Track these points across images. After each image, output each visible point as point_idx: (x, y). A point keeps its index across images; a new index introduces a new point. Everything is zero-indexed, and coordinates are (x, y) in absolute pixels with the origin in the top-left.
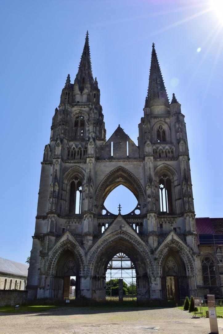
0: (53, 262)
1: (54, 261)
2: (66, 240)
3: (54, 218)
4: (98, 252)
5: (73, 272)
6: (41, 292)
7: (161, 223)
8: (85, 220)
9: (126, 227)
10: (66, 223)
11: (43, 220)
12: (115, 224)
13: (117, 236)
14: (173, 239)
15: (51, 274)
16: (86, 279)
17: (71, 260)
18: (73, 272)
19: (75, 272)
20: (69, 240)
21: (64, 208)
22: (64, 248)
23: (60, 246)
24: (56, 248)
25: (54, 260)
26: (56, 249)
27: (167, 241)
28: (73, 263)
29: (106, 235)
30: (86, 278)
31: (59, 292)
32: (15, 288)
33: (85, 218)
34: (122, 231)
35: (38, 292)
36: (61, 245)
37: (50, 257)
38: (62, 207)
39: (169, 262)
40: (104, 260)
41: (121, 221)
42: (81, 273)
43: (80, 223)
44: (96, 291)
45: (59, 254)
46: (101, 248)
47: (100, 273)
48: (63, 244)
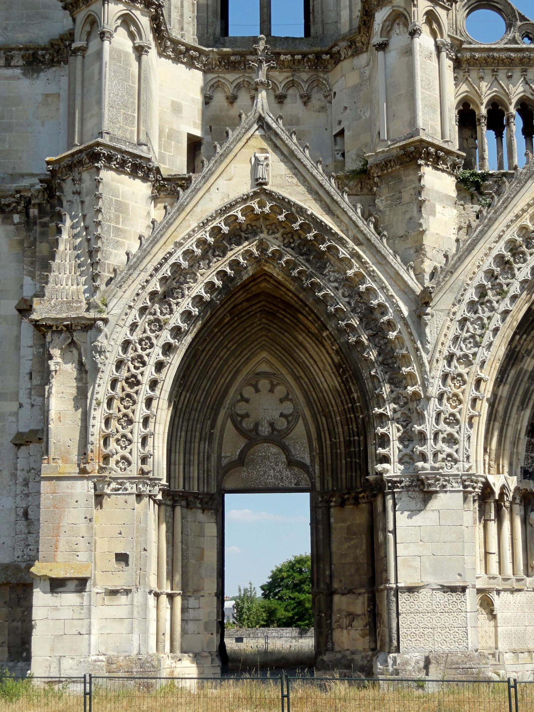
0: (149, 371)
1: (160, 366)
2: (245, 199)
3: (132, 36)
5: (291, 463)
6: (66, 614)
8: (383, 47)
11: (24, 74)
15: (133, 471)
16: (435, 503)
17: (264, 368)
18: (283, 458)
19: (307, 461)
20: (270, 195)
22: (234, 264)
23: (201, 242)
24: (166, 259)
25: (157, 354)
26: (166, 270)
28: (280, 390)
32: (424, 287)
33: (387, 30)
35: (37, 614)
36: (211, 240)
37: (124, 333)
42: (385, 459)
43: (317, 98)
44: (494, 596)
45: (195, 311)
48: (226, 229)
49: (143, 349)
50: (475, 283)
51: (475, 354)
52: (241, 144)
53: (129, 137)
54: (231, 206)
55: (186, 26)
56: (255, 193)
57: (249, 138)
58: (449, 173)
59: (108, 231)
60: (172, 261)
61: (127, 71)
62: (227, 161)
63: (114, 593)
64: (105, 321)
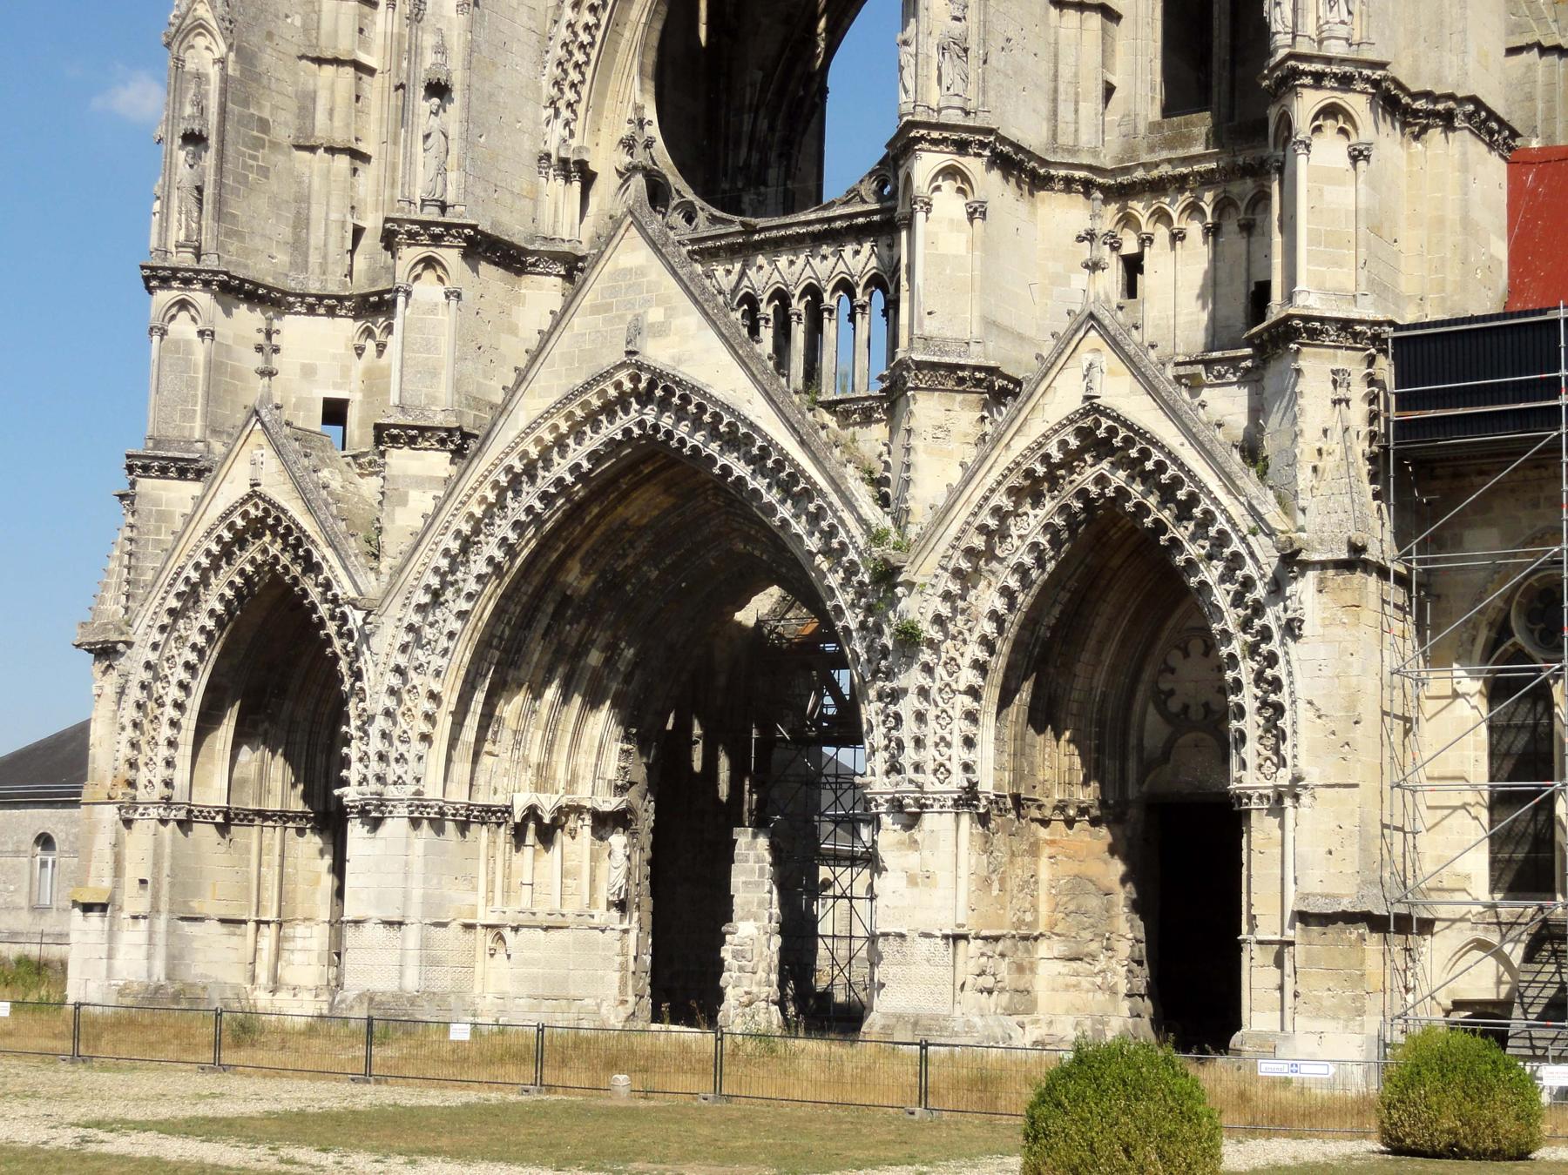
2: (244, 502)
4: (472, 586)
7: (1130, 246)
9: (676, 323)
10: (360, 351)
12: (595, 309)
13: (611, 430)
14: (1092, 407)
21: (334, 216)
27: (1036, 429)
29: (523, 423)
30: (375, 824)
31: (299, 944)
34: (645, 377)
37: (146, 654)
38: (317, 212)
39: (1176, 658)
40: (595, 658)
41: (641, 272)
44: (507, 933)
46: (492, 549)
47: (561, 775)
49: (170, 668)
50: (423, 584)
51: (429, 663)
52: (241, 442)
53: (187, 434)
54: (230, 512)
55: (331, 268)
56: (250, 497)
57: (248, 436)
58: (437, 450)
59: (146, 545)
60: (183, 575)
61: (187, 361)
62: (229, 462)
63: (135, 918)
64: (129, 644)
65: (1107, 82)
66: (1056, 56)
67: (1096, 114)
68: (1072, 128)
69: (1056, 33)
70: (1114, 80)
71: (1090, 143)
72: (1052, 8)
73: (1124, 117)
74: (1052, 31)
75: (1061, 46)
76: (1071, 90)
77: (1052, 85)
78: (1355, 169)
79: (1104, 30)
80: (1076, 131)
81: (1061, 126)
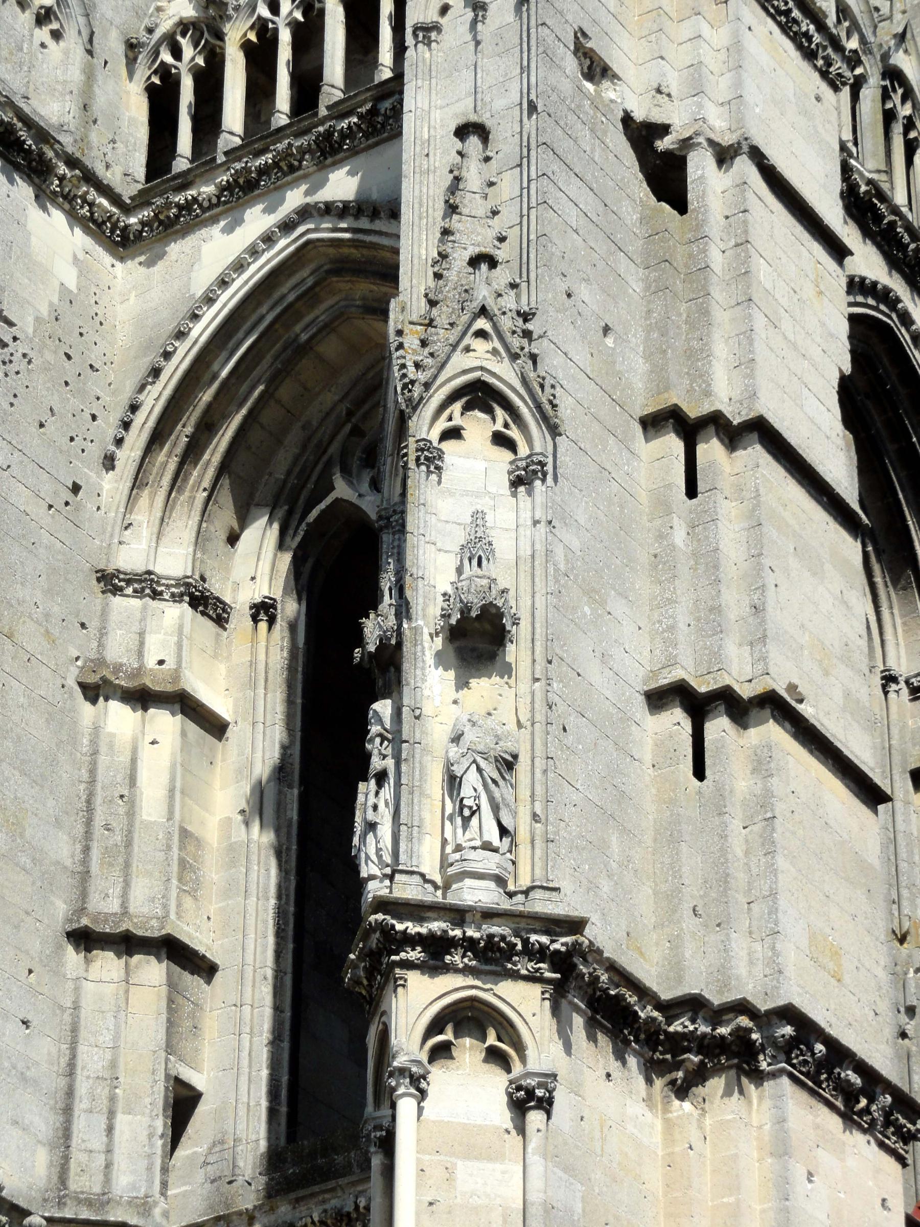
65: (178, 1081)
66: (75, 1030)
67: (151, 1136)
68: (101, 1160)
69: (77, 989)
70: (198, 1080)
71: (134, 1187)
72: (70, 949)
73: (214, 1145)
74: (70, 985)
75: (83, 1013)
76: (103, 1092)
77: (63, 1082)
78: (521, 1130)
79: (172, 985)
80: (108, 1166)
81: (77, 1157)
